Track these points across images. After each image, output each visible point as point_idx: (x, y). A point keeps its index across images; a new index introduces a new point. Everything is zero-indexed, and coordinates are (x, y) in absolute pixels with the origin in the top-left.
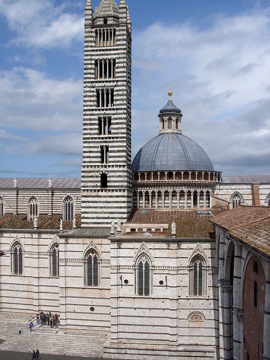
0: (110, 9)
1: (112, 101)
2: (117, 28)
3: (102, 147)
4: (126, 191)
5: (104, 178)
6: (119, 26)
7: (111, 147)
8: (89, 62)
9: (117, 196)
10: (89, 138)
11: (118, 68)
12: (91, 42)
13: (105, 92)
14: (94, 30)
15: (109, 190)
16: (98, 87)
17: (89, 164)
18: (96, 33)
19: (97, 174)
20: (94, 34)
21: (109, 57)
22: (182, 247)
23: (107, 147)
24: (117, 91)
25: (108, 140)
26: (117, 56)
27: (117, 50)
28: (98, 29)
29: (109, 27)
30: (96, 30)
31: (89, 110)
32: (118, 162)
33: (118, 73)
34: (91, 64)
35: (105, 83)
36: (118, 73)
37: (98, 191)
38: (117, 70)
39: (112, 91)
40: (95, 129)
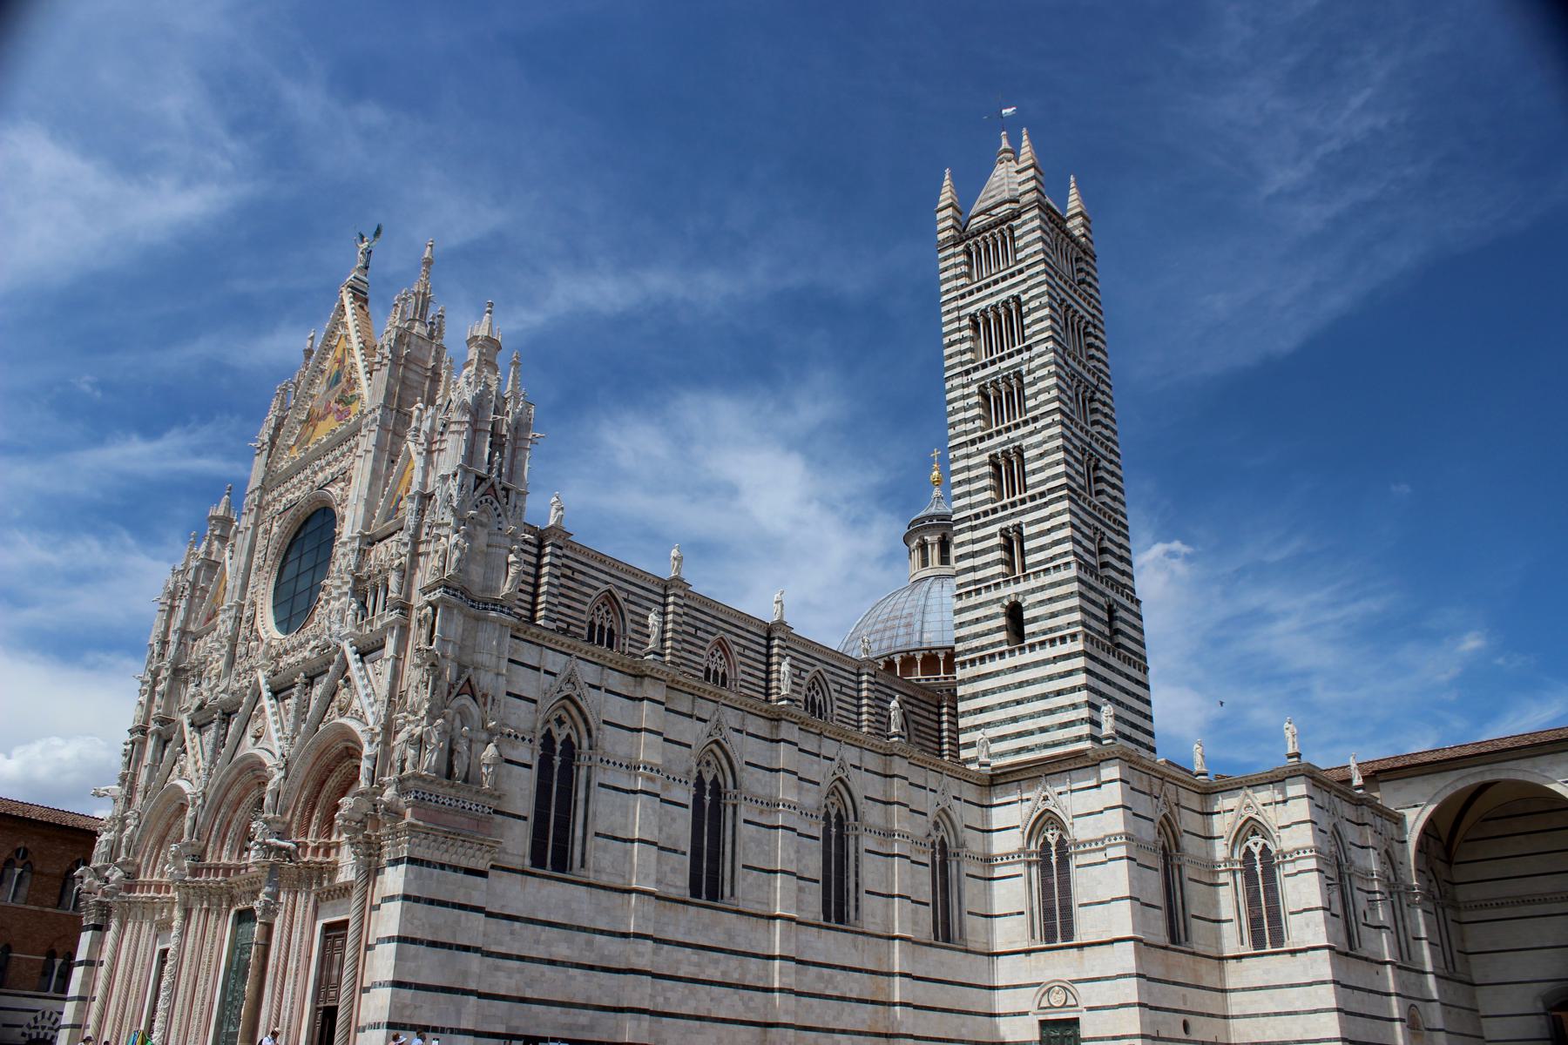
0: (1002, 189)
2: (1015, 223)
3: (1004, 533)
4: (1080, 637)
5: (1015, 613)
6: (1019, 216)
7: (1029, 524)
8: (956, 325)
9: (1055, 660)
10: (968, 518)
11: (1031, 311)
12: (957, 277)
13: (1002, 386)
14: (961, 248)
15: (1032, 647)
16: (983, 378)
17: (972, 588)
18: (970, 255)
19: (997, 609)
20: (962, 258)
21: (1004, 296)
22: (1290, 794)
23: (1018, 528)
24: (1029, 372)
26: (1024, 287)
28: (971, 243)
29: (996, 225)
30: (968, 247)
34: (960, 330)
35: (998, 365)
37: (1002, 654)
38: (1027, 321)
40: (985, 489)
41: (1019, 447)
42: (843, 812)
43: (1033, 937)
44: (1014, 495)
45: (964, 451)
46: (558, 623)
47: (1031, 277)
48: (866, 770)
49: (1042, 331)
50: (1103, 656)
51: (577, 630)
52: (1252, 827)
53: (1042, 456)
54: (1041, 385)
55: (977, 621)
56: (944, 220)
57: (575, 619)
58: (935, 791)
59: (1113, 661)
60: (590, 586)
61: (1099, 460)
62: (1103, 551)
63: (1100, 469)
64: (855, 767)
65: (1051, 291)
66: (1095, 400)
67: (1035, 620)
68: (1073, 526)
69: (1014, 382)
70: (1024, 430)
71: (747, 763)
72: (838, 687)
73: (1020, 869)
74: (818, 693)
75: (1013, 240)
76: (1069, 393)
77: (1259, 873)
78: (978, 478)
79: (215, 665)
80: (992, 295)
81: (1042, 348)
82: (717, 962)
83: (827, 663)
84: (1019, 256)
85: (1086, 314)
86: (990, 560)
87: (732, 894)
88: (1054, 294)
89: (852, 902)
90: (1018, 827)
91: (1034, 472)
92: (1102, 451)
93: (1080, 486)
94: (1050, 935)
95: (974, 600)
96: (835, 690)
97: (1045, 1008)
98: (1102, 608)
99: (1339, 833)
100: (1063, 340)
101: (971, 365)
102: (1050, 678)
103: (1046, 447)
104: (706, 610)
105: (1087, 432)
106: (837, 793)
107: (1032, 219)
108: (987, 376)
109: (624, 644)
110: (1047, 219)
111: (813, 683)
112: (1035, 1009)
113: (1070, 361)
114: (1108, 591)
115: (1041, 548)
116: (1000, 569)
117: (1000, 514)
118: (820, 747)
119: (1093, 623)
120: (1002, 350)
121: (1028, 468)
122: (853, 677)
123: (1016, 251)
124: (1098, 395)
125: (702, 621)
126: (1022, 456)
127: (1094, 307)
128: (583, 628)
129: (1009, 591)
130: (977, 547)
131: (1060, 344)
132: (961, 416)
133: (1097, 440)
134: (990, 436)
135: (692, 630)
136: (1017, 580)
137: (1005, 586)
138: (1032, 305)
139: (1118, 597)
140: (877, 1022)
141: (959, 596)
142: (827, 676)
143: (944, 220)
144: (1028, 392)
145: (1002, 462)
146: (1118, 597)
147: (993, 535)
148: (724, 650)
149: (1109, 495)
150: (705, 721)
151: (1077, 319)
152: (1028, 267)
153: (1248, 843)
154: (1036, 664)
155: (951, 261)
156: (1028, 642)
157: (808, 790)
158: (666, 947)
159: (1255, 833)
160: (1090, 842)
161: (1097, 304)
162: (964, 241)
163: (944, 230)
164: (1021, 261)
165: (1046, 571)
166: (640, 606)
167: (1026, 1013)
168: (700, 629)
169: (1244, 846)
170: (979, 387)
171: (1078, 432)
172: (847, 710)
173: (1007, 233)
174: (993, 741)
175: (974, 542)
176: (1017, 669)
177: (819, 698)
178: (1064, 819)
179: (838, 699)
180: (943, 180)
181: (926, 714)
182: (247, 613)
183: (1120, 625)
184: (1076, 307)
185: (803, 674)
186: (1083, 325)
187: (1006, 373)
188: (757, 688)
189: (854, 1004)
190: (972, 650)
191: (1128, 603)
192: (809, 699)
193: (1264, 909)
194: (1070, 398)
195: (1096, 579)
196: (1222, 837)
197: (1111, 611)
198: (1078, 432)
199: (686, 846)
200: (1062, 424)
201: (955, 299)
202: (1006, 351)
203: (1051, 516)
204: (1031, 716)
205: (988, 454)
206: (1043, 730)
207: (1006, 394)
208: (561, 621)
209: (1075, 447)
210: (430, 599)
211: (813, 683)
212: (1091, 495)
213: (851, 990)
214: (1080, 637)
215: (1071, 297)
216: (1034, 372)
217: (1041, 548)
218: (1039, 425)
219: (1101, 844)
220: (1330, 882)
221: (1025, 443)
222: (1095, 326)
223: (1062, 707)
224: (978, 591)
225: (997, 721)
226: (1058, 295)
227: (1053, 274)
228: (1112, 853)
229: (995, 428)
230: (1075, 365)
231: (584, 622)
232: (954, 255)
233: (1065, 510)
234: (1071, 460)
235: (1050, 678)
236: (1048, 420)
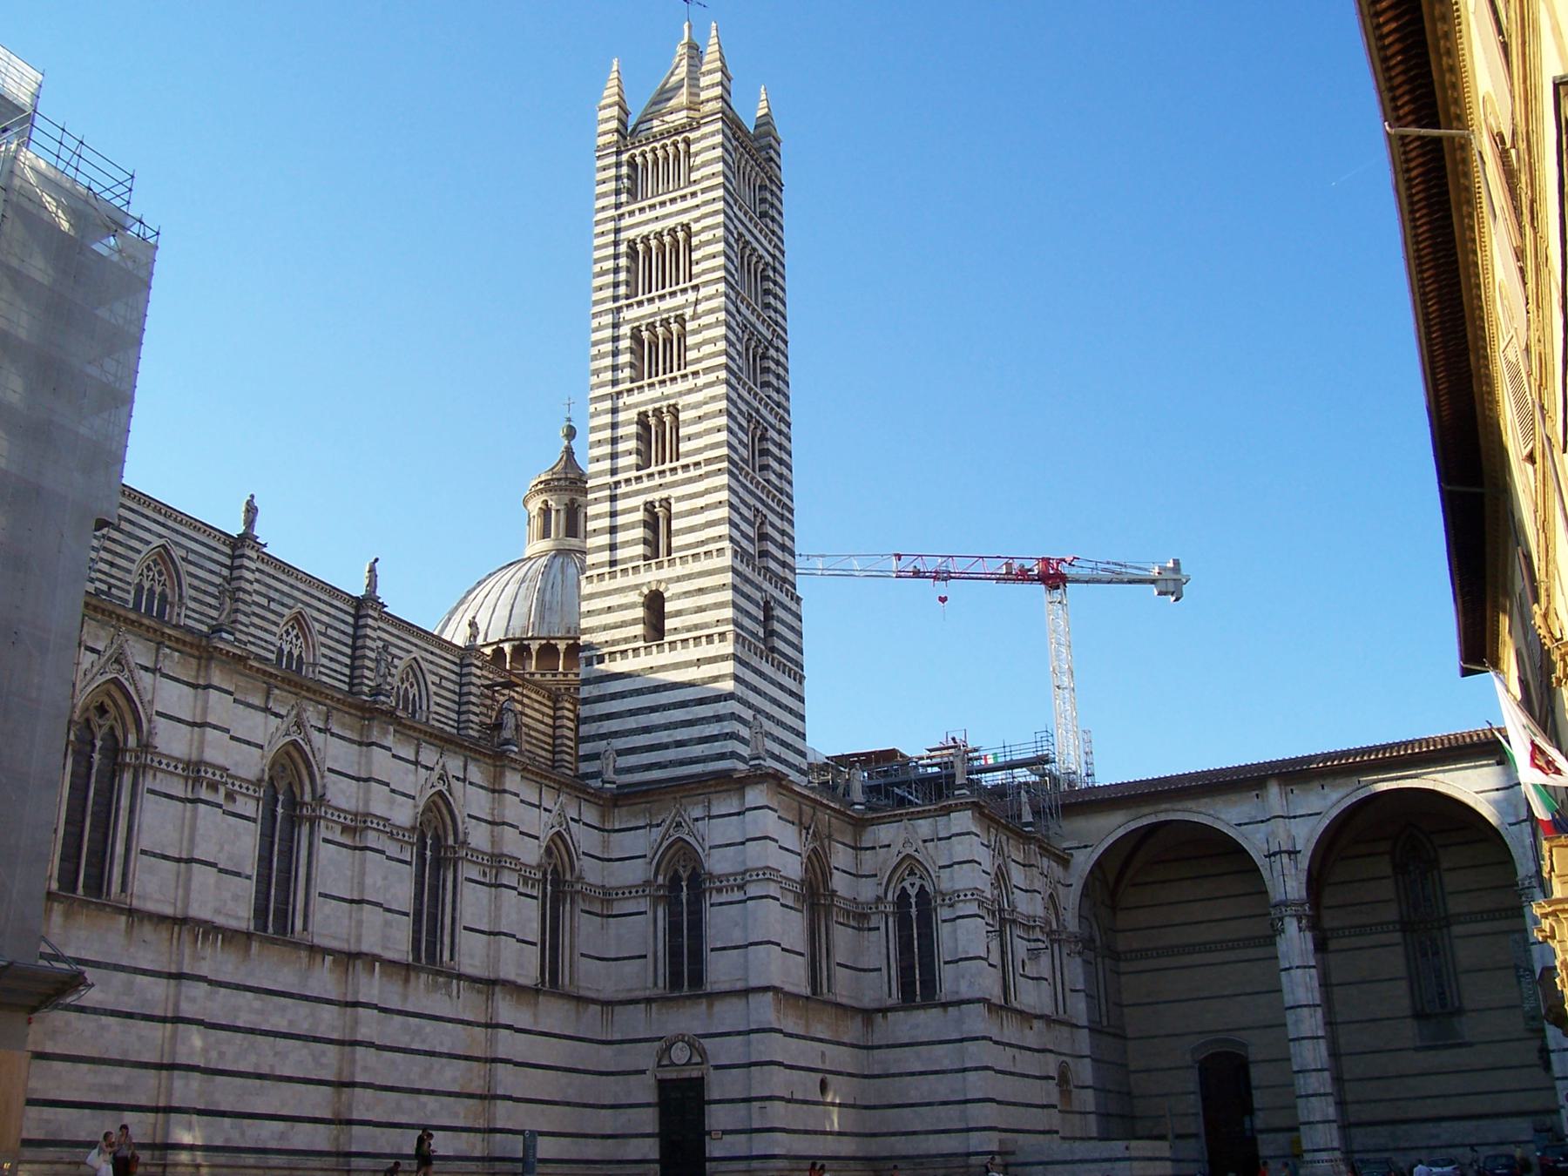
2: (692, 136)
5: (655, 603)
7: (680, 499)
14: (625, 157)
16: (637, 319)
20: (624, 170)
21: (671, 223)
23: (666, 502)
25: (669, 478)
26: (696, 214)
27: (694, 194)
30: (633, 157)
38: (695, 256)
39: (681, 320)
41: (674, 406)
42: (441, 832)
43: (656, 984)
44: (663, 463)
46: (98, 584)
47: (706, 203)
48: (471, 783)
49: (713, 270)
50: (755, 661)
51: (120, 594)
52: (910, 864)
54: (707, 334)
56: (607, 120)
57: (120, 580)
58: (550, 811)
59: (766, 668)
60: (141, 540)
61: (767, 430)
62: (763, 537)
63: (767, 440)
64: (458, 779)
65: (728, 222)
66: (768, 358)
67: (679, 613)
68: (731, 505)
69: (674, 327)
70: (681, 386)
71: (330, 770)
72: (437, 680)
73: (644, 905)
74: (412, 686)
75: (688, 154)
76: (739, 347)
77: (914, 917)
81: (711, 290)
82: (284, 1009)
83: (426, 650)
85: (765, 254)
86: (629, 538)
87: (305, 929)
88: (732, 227)
89: (447, 940)
90: (645, 856)
92: (771, 418)
93: (742, 459)
94: (675, 980)
95: (608, 584)
96: (433, 683)
97: (667, 1066)
98: (758, 605)
99: (1003, 875)
100: (737, 283)
101: (623, 302)
104: (283, 577)
105: (756, 394)
106: (434, 809)
107: (713, 134)
108: (643, 317)
109: (179, 615)
110: (731, 136)
111: (408, 674)
112: (649, 1063)
113: (743, 308)
114: (766, 585)
115: (692, 529)
117: (646, 484)
118: (417, 753)
119: (747, 622)
120: (664, 287)
122: (456, 669)
123: (691, 170)
124: (772, 352)
125: (276, 590)
126: (677, 418)
127: (776, 246)
128: (129, 592)
129: (650, 577)
131: (733, 288)
133: (766, 405)
135: (264, 602)
136: (660, 566)
137: (646, 571)
138: (705, 237)
139: (777, 593)
140: (471, 1080)
142: (424, 665)
143: (607, 120)
144: (690, 341)
146: (777, 593)
147: (636, 509)
148: (301, 628)
149: (774, 472)
150: (281, 717)
151: (754, 259)
152: (704, 191)
153: (903, 884)
156: (667, 639)
157: (401, 805)
158: (223, 990)
159: (912, 873)
160: (727, 876)
161: (779, 244)
162: (629, 150)
163: (605, 133)
166: (201, 567)
167: (643, 1072)
168: (274, 600)
169: (900, 886)
170: (633, 329)
171: (745, 394)
172: (447, 708)
173: (681, 146)
174: (620, 753)
177: (413, 691)
178: (700, 850)
179: (436, 694)
180: (609, 71)
181: (539, 716)
183: (777, 626)
184: (756, 245)
185: (396, 661)
186: (761, 267)
187: (665, 316)
188: (339, 677)
189: (444, 1060)
191: (787, 601)
192: (402, 693)
193: (916, 958)
194: (739, 353)
195: (754, 570)
196: (876, 875)
197: (767, 609)
198: (745, 394)
199: (251, 867)
200: (727, 382)
202: (668, 289)
203: (707, 492)
205: (636, 411)
206: (680, 744)
207: (664, 340)
208: (101, 581)
209: (740, 412)
211: (408, 674)
212: (754, 471)
213: (442, 1044)
214: (730, 637)
215: (750, 231)
216: (699, 318)
217: (692, 529)
220: (990, 929)
221: (682, 402)
222: (775, 270)
223: (703, 718)
224: (613, 575)
225: (626, 731)
226: (736, 228)
227: (732, 202)
229: (647, 381)
230: (748, 313)
231: (129, 584)
233: (723, 486)
234: (735, 428)
236: (712, 377)
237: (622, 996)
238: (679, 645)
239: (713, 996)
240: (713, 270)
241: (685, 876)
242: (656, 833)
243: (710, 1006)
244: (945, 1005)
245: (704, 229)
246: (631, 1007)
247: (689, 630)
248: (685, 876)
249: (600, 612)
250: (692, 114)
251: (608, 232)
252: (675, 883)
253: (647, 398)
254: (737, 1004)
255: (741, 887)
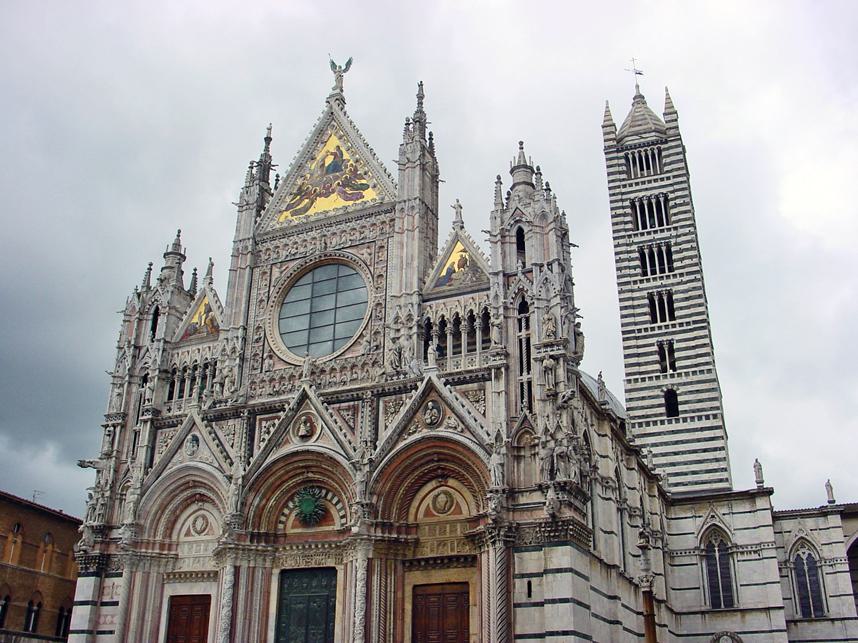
1: (670, 261)
2: (663, 146)
3: (660, 345)
5: (671, 398)
6: (666, 142)
7: (678, 341)
8: (620, 204)
9: (702, 429)
10: (633, 331)
11: (676, 206)
12: (620, 173)
13: (655, 250)
14: (622, 154)
15: (685, 420)
19: (657, 392)
20: (623, 161)
21: (656, 192)
25: (671, 330)
26: (671, 189)
27: (668, 178)
31: (628, 283)
32: (696, 365)
33: (675, 214)
34: (623, 208)
35: (653, 235)
36: (675, 214)
37: (662, 422)
39: (669, 247)
40: (645, 314)
44: (663, 319)
45: (628, 287)
49: (685, 220)
52: (803, 542)
53: (687, 299)
54: (685, 254)
55: (643, 398)
67: (686, 402)
69: (664, 249)
70: (672, 280)
78: (639, 306)
79: (225, 372)
80: (646, 189)
84: (666, 169)
91: (681, 308)
94: (715, 603)
95: (640, 385)
101: (631, 232)
102: (699, 440)
103: (690, 294)
108: (645, 242)
116: (658, 367)
121: (676, 305)
129: (668, 381)
130: (641, 351)
132: (626, 264)
134: (648, 280)
136: (672, 376)
138: (678, 201)
141: (629, 381)
144: (674, 257)
145: (656, 298)
147: (652, 345)
152: (674, 177)
154: (688, 431)
155: (615, 162)
160: (747, 546)
164: (667, 172)
165: (694, 373)
173: (656, 152)
175: (638, 347)
176: (673, 432)
182: (252, 335)
190: (639, 417)
201: (619, 187)
204: (685, 463)
206: (694, 473)
210: (552, 353)
216: (680, 244)
218: (685, 278)
219: (758, 549)
221: (674, 289)
224: (643, 380)
228: (765, 554)
232: (618, 158)
235: (699, 440)
236: (692, 277)
237: (685, 610)
238: (689, 420)
239: (744, 611)
240: (685, 220)
241: (716, 545)
242: (700, 521)
243: (743, 617)
244: (833, 620)
245: (676, 198)
246: (692, 616)
247: (693, 411)
248: (716, 545)
249: (638, 399)
250: (657, 134)
251: (618, 194)
252: (710, 548)
253: (654, 284)
254: (763, 615)
255: (755, 552)
